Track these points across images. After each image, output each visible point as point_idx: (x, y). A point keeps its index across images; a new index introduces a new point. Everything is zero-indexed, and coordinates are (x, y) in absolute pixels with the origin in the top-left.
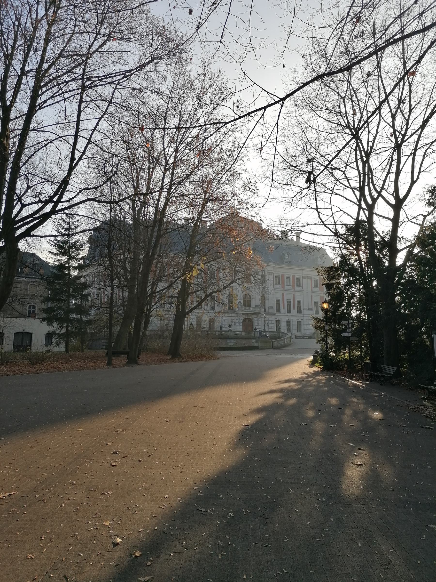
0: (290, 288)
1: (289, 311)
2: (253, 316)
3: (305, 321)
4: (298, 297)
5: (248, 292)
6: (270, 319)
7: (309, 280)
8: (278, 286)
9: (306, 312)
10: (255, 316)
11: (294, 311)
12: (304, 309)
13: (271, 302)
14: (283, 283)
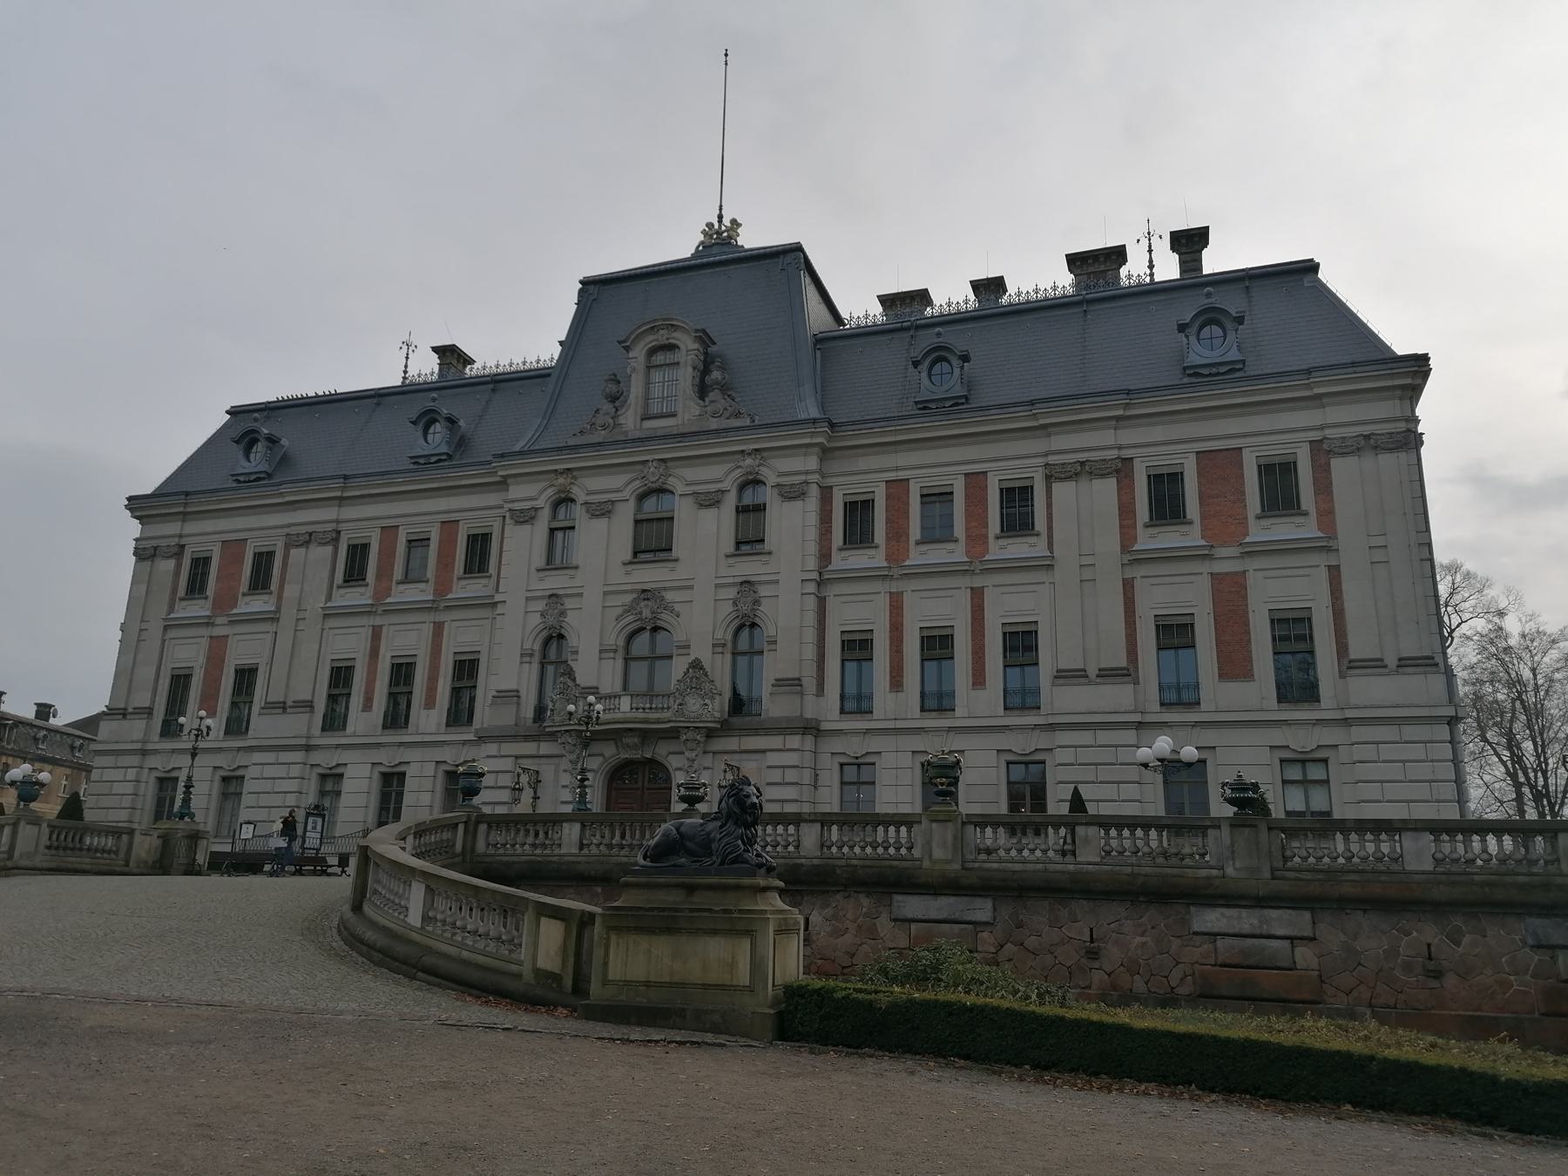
0: (955, 553)
1: (937, 701)
2: (661, 751)
5: (646, 613)
6: (773, 759)
7: (1107, 489)
8: (860, 559)
10: (673, 746)
11: (979, 702)
12: (1064, 676)
14: (897, 532)
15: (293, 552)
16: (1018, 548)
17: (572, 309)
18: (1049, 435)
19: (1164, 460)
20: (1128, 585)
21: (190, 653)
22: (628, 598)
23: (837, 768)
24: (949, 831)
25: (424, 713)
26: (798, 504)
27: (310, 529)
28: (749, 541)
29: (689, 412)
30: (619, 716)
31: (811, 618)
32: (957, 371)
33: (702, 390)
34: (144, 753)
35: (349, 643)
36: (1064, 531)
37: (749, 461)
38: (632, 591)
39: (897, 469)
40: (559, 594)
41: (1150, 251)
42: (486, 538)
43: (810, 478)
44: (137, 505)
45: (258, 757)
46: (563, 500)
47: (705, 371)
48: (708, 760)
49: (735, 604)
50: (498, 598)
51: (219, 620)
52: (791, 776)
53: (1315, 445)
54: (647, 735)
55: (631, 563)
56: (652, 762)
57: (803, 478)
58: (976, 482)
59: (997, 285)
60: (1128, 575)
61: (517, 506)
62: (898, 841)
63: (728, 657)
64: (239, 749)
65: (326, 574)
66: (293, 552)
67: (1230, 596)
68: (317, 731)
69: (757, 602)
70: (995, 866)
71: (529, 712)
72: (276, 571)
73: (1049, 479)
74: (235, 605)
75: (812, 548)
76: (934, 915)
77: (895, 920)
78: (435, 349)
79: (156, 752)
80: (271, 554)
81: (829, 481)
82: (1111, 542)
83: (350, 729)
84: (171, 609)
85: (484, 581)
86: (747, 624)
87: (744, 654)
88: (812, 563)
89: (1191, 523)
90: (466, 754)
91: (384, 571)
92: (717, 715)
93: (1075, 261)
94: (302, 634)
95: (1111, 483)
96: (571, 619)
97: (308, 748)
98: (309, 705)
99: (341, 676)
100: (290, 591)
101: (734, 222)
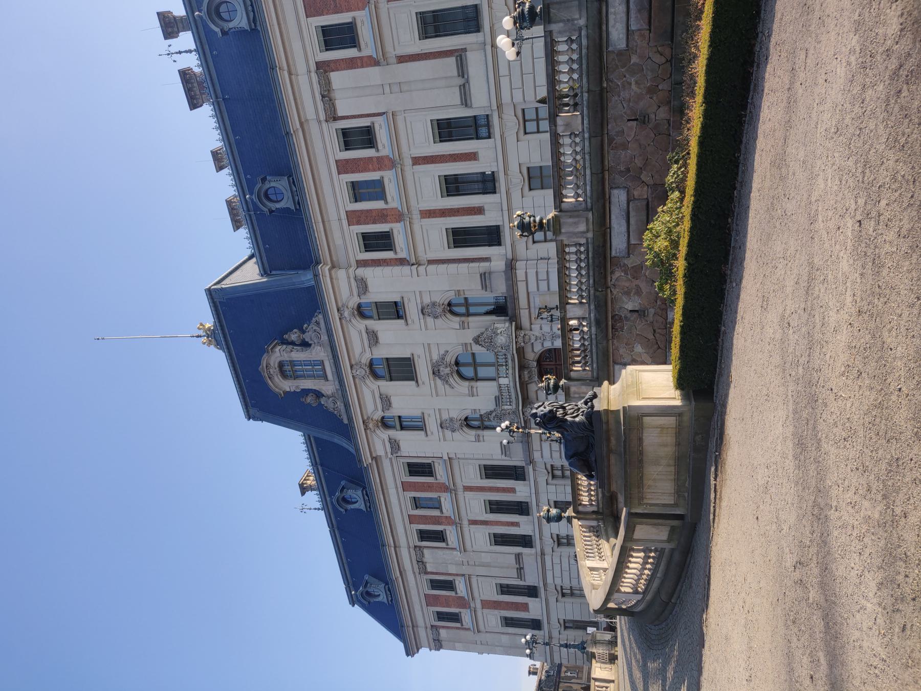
1: (487, 184)
3: (518, 97)
5: (447, 370)
6: (533, 287)
7: (338, 78)
8: (400, 240)
10: (528, 349)
11: (485, 156)
12: (465, 101)
14: (381, 216)
15: (429, 569)
16: (382, 136)
17: (266, 424)
18: (307, 120)
19: (314, 40)
20: (402, 59)
21: (493, 618)
22: (439, 382)
23: (536, 245)
24: (566, 220)
25: (518, 494)
27: (415, 562)
28: (394, 310)
29: (319, 353)
30: (512, 384)
31: (442, 268)
33: (305, 345)
35: (480, 538)
37: (346, 314)
38: (434, 380)
39: (340, 219)
40: (440, 424)
41: (180, 52)
42: (410, 465)
43: (352, 276)
44: (409, 652)
45: (550, 580)
46: (385, 423)
47: (293, 343)
49: (436, 317)
50: (446, 457)
51: (472, 605)
52: (543, 276)
54: (522, 367)
55: (417, 382)
56: (539, 361)
57: (352, 280)
58: (344, 167)
59: (215, 154)
60: (395, 60)
61: (389, 450)
62: (576, 253)
63: (471, 319)
64: (546, 590)
65: (440, 552)
66: (429, 569)
68: (532, 551)
69: (434, 304)
70: (588, 188)
73: (335, 119)
74: (463, 598)
75: (397, 270)
76: (624, 228)
77: (629, 254)
78: (303, 494)
79: (550, 632)
80: (432, 581)
81: (354, 263)
82: (372, 74)
83: (530, 533)
84: (468, 629)
85: (436, 465)
86: (450, 309)
87: (467, 310)
88: (406, 269)
89: (354, 18)
90: (541, 468)
92: (507, 324)
93: (194, 104)
95: (335, 76)
96: (454, 414)
97: (543, 554)
98: (518, 556)
99: (501, 540)
100: (452, 569)
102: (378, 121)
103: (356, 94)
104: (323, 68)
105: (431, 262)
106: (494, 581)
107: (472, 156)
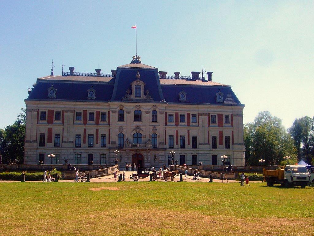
4: (194, 132)
5: (138, 130)
6: (160, 154)
9: (200, 146)
10: (145, 152)
11: (189, 146)
12: (200, 144)
13: (161, 139)
20: (209, 132)
22: (134, 128)
25: (96, 144)
26: (162, 115)
29: (143, 97)
32: (185, 96)
33: (145, 94)
34: (37, 149)
36: (201, 123)
44: (25, 100)
45: (63, 151)
48: (150, 154)
49: (153, 130)
52: (163, 157)
53: (232, 115)
57: (163, 111)
58: (188, 114)
67: (221, 133)
71: (117, 146)
72: (61, 117)
86: (154, 134)
91: (85, 118)
93: (192, 73)
94: (70, 130)
96: (125, 130)
97: (74, 150)
98: (72, 142)
100: (65, 121)
101: (139, 57)
102: (197, 124)
103: (203, 119)
104: (208, 115)
105: (166, 130)
106: (61, 133)
107: (189, 144)
